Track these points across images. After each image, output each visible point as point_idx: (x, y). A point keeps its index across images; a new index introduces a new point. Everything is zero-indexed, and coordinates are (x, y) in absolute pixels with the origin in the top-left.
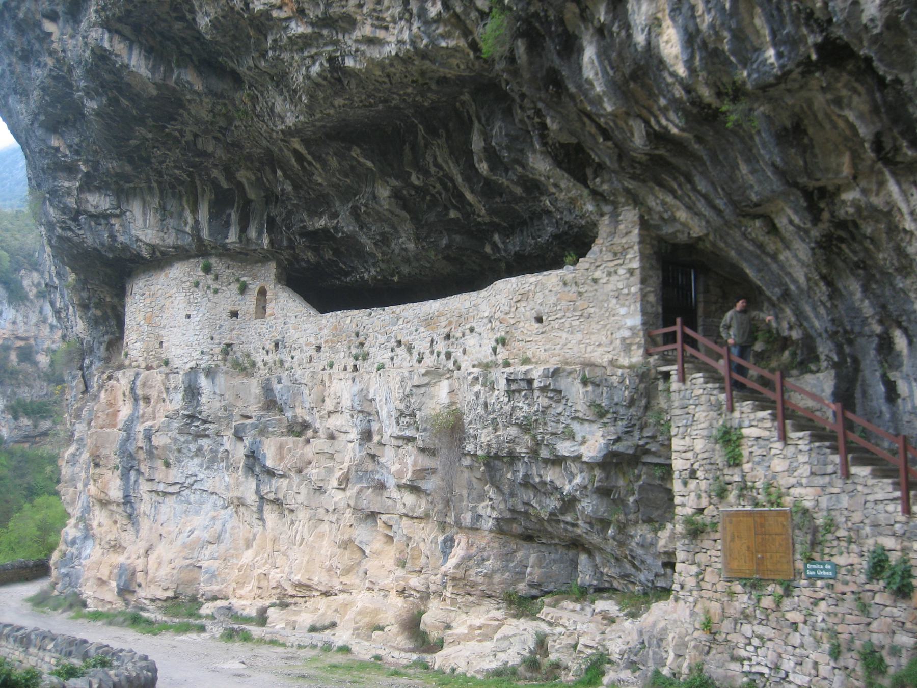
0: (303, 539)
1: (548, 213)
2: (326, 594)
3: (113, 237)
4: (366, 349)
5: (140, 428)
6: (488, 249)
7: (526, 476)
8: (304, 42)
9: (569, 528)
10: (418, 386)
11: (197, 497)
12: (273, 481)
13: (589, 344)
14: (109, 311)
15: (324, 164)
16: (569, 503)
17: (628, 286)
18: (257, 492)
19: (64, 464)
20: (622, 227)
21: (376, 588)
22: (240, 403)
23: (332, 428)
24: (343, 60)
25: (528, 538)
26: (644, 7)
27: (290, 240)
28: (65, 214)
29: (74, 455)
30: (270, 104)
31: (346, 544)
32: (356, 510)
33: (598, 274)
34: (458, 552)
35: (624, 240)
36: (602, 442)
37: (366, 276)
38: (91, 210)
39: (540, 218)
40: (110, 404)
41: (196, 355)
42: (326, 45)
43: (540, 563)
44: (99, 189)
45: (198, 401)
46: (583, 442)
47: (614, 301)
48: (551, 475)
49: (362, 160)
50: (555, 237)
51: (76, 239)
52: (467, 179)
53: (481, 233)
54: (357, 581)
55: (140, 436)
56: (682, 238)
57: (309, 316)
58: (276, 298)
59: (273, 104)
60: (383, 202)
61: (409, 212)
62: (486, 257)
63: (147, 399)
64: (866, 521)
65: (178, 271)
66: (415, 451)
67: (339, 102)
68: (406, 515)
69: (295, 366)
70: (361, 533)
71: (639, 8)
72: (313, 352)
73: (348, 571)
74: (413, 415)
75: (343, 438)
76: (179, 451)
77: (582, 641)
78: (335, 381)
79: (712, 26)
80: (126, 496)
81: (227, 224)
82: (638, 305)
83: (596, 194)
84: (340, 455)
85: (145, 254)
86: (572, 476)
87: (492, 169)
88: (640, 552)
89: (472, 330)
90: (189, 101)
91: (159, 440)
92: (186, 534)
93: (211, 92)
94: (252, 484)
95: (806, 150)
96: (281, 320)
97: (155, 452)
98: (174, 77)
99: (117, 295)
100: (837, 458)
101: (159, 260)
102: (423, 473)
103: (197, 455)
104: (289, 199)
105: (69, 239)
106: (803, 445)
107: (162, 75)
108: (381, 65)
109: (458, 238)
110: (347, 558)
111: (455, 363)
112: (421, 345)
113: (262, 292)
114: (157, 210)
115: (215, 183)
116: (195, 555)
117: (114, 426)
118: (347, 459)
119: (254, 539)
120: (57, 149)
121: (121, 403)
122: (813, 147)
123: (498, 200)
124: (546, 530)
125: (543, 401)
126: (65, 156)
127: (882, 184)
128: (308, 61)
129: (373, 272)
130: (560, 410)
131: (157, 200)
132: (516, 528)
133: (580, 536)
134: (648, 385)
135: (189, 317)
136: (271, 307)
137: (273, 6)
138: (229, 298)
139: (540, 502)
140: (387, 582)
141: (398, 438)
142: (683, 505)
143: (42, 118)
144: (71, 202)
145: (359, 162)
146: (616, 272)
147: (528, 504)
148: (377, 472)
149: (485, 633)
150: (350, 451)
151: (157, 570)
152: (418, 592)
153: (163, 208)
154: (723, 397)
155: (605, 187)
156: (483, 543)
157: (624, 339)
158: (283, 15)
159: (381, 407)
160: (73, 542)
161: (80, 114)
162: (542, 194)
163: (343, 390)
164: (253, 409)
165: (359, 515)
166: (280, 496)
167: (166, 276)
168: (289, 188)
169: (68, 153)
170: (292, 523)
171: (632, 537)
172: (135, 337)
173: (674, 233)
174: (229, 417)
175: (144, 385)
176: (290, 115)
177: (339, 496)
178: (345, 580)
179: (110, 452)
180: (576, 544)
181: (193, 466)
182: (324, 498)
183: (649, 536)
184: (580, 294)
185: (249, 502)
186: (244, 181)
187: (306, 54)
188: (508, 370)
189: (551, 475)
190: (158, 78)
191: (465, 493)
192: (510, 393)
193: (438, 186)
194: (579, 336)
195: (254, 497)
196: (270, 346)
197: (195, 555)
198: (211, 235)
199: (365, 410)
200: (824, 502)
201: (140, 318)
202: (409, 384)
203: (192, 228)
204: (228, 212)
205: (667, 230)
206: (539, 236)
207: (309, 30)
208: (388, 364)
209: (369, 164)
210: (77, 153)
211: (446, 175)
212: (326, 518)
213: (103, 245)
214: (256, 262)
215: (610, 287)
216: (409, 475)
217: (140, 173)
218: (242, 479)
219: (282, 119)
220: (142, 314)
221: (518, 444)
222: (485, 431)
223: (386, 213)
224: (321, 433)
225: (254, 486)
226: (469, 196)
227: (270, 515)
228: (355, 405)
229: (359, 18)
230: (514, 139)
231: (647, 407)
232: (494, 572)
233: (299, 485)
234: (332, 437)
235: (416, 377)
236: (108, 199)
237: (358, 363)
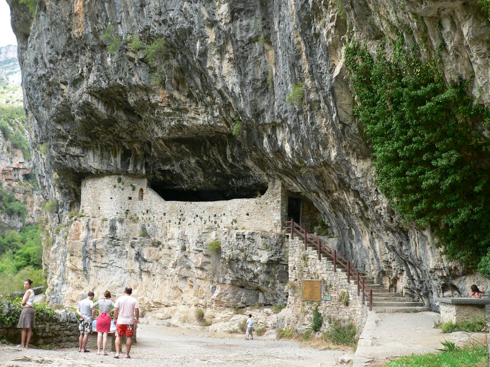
1: (252, 176)
2: (167, 306)
3: (80, 165)
4: (184, 216)
5: (91, 241)
6: (230, 183)
7: (242, 266)
8: (169, 114)
11: (114, 268)
12: (146, 264)
14: (72, 191)
15: (171, 149)
16: (256, 276)
17: (277, 206)
18: (140, 268)
19: (51, 253)
21: (186, 304)
23: (170, 245)
26: (281, 135)
27: (153, 171)
29: (56, 249)
31: (175, 288)
32: (179, 275)
33: (267, 201)
34: (218, 291)
36: (267, 256)
37: (183, 187)
38: (72, 153)
39: (249, 177)
40: (76, 231)
41: (115, 214)
44: (75, 146)
46: (261, 256)
48: (250, 266)
50: (254, 184)
51: (63, 164)
52: (224, 161)
54: (179, 302)
55: (91, 244)
56: (296, 191)
62: (230, 186)
63: (94, 230)
65: (106, 179)
67: (180, 133)
70: (181, 284)
72: (163, 216)
74: (202, 243)
75: (174, 249)
77: (259, 321)
79: (298, 149)
80: (84, 268)
81: (128, 163)
85: (93, 172)
86: (257, 267)
88: (279, 292)
89: (224, 214)
91: (99, 246)
94: (137, 264)
95: (324, 181)
98: (115, 113)
100: (333, 266)
101: (99, 175)
102: (205, 263)
104: (155, 158)
105: (60, 164)
106: (325, 261)
109: (219, 179)
112: (206, 218)
113: (142, 190)
114: (99, 156)
115: (124, 148)
117: (78, 239)
118: (176, 256)
120: (60, 130)
121: (81, 230)
125: (248, 242)
127: (343, 193)
129: (186, 186)
131: (99, 152)
132: (238, 284)
134: (282, 240)
136: (145, 196)
137: (159, 102)
138: (128, 191)
139: (246, 275)
140: (190, 302)
141: (196, 250)
142: (291, 278)
143: (55, 118)
144: (63, 150)
147: (243, 276)
149: (226, 319)
150: (177, 254)
154: (304, 245)
155: (271, 173)
156: (226, 288)
157: (275, 224)
158: (162, 105)
160: (57, 285)
161: (72, 118)
165: (180, 277)
167: (102, 181)
168: (156, 155)
170: (154, 280)
174: (128, 239)
175: (92, 224)
177: (173, 270)
179: (78, 251)
180: (258, 289)
181: (112, 257)
182: (166, 271)
183: (282, 287)
184: (262, 207)
185: (136, 271)
186: (136, 148)
188: (237, 231)
189: (250, 266)
190: (109, 113)
191: (221, 271)
192: (238, 239)
193: (213, 161)
194: (261, 221)
195: (138, 270)
196: (145, 212)
199: (183, 239)
201: (90, 196)
202: (201, 232)
203: (114, 164)
205: (290, 189)
207: (171, 111)
208: (193, 223)
209: (188, 150)
210: (69, 132)
211: (216, 158)
212: (167, 278)
213: (75, 167)
214: (139, 178)
216: (200, 264)
218: (133, 262)
219: (157, 134)
220: (90, 195)
224: (165, 246)
225: (138, 266)
226: (224, 166)
227: (145, 277)
230: (241, 154)
231: (281, 246)
232: (230, 298)
233: (157, 266)
234: (170, 248)
237: (181, 222)
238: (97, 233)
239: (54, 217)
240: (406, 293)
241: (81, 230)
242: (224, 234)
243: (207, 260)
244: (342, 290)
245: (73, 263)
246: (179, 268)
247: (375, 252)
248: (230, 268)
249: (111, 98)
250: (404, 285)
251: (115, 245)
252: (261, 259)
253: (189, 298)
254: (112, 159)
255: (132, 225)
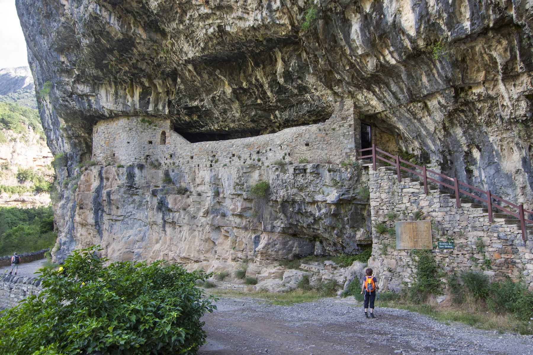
0: (186, 238)
2: (196, 262)
3: (90, 105)
4: (216, 158)
7: (299, 209)
9: (315, 231)
10: (245, 173)
12: (171, 214)
13: (331, 155)
16: (317, 220)
17: (349, 132)
18: (163, 219)
20: (345, 107)
21: (221, 258)
22: (154, 181)
24: (225, 27)
25: (294, 235)
27: (178, 111)
28: (65, 94)
29: (64, 205)
30: (181, 47)
31: (207, 240)
32: (212, 225)
33: (335, 126)
35: (346, 113)
36: (337, 195)
37: (212, 128)
38: (80, 93)
40: (87, 181)
41: (133, 159)
42: (217, 19)
43: (299, 246)
45: (134, 179)
46: (328, 195)
47: (342, 137)
49: (220, 76)
53: (270, 110)
58: (171, 136)
59: (183, 47)
60: (228, 95)
61: (238, 101)
62: (271, 121)
64: (469, 225)
65: (123, 122)
66: (242, 200)
67: (219, 47)
68: (236, 227)
69: (181, 165)
70: (213, 235)
71: (391, 5)
73: (207, 252)
76: (124, 201)
78: (201, 172)
81: (148, 102)
82: (353, 139)
83: (335, 94)
84: (204, 202)
85: (106, 114)
87: (285, 81)
90: (138, 43)
92: (127, 238)
93: (151, 39)
97: (112, 202)
98: (132, 31)
99: (88, 133)
101: (113, 116)
102: (244, 209)
103: (132, 203)
105: (66, 106)
106: (437, 195)
107: (126, 30)
108: (243, 30)
109: (260, 112)
110: (207, 246)
113: (164, 133)
116: (131, 247)
117: (89, 191)
118: (207, 204)
119: (160, 239)
120: (63, 62)
122: (468, 69)
123: (283, 95)
124: (303, 232)
125: (310, 178)
126: (67, 66)
128: (207, 27)
129: (216, 126)
130: (318, 181)
131: (113, 90)
132: (291, 231)
133: (319, 234)
135: (129, 143)
144: (69, 88)
145: (218, 77)
146: (343, 126)
147: (298, 221)
148: (221, 209)
150: (208, 201)
151: (112, 254)
152: (241, 259)
153: (116, 93)
155: (340, 90)
156: (275, 238)
157: (346, 153)
159: (225, 182)
160: (65, 243)
161: (78, 46)
162: (307, 93)
163: (205, 175)
164: (160, 184)
165: (213, 227)
166: (175, 220)
169: (69, 64)
170: (180, 232)
171: (345, 234)
172: (100, 151)
173: (368, 111)
174: (149, 187)
175: (106, 172)
176: (191, 52)
177: (203, 220)
178: (206, 255)
179: (89, 203)
181: (130, 208)
184: (327, 134)
185: (158, 223)
187: (206, 23)
189: (309, 209)
191: (268, 217)
194: (326, 151)
196: (169, 156)
197: (131, 247)
198: (140, 107)
199: (216, 183)
200: (447, 218)
204: (148, 97)
206: (300, 112)
207: (210, 11)
208: (229, 164)
215: (340, 132)
216: (239, 210)
217: (106, 77)
218: (155, 213)
219: (186, 54)
221: (297, 196)
222: (282, 190)
223: (228, 100)
224: (194, 193)
226: (269, 94)
227: (169, 230)
228: (212, 181)
229: (235, 8)
230: (300, 67)
232: (279, 250)
233: (184, 216)
234: (199, 195)
235: (245, 169)
236: (88, 88)
237: (213, 164)
238: (111, 182)
239: (63, 170)
241: (93, 180)
242: (275, 171)
243: (249, 205)
244: (475, 233)
246: (211, 217)
248: (283, 213)
251: (133, 195)
252: (328, 198)
253: (224, 251)
254: (129, 97)
255: (153, 171)
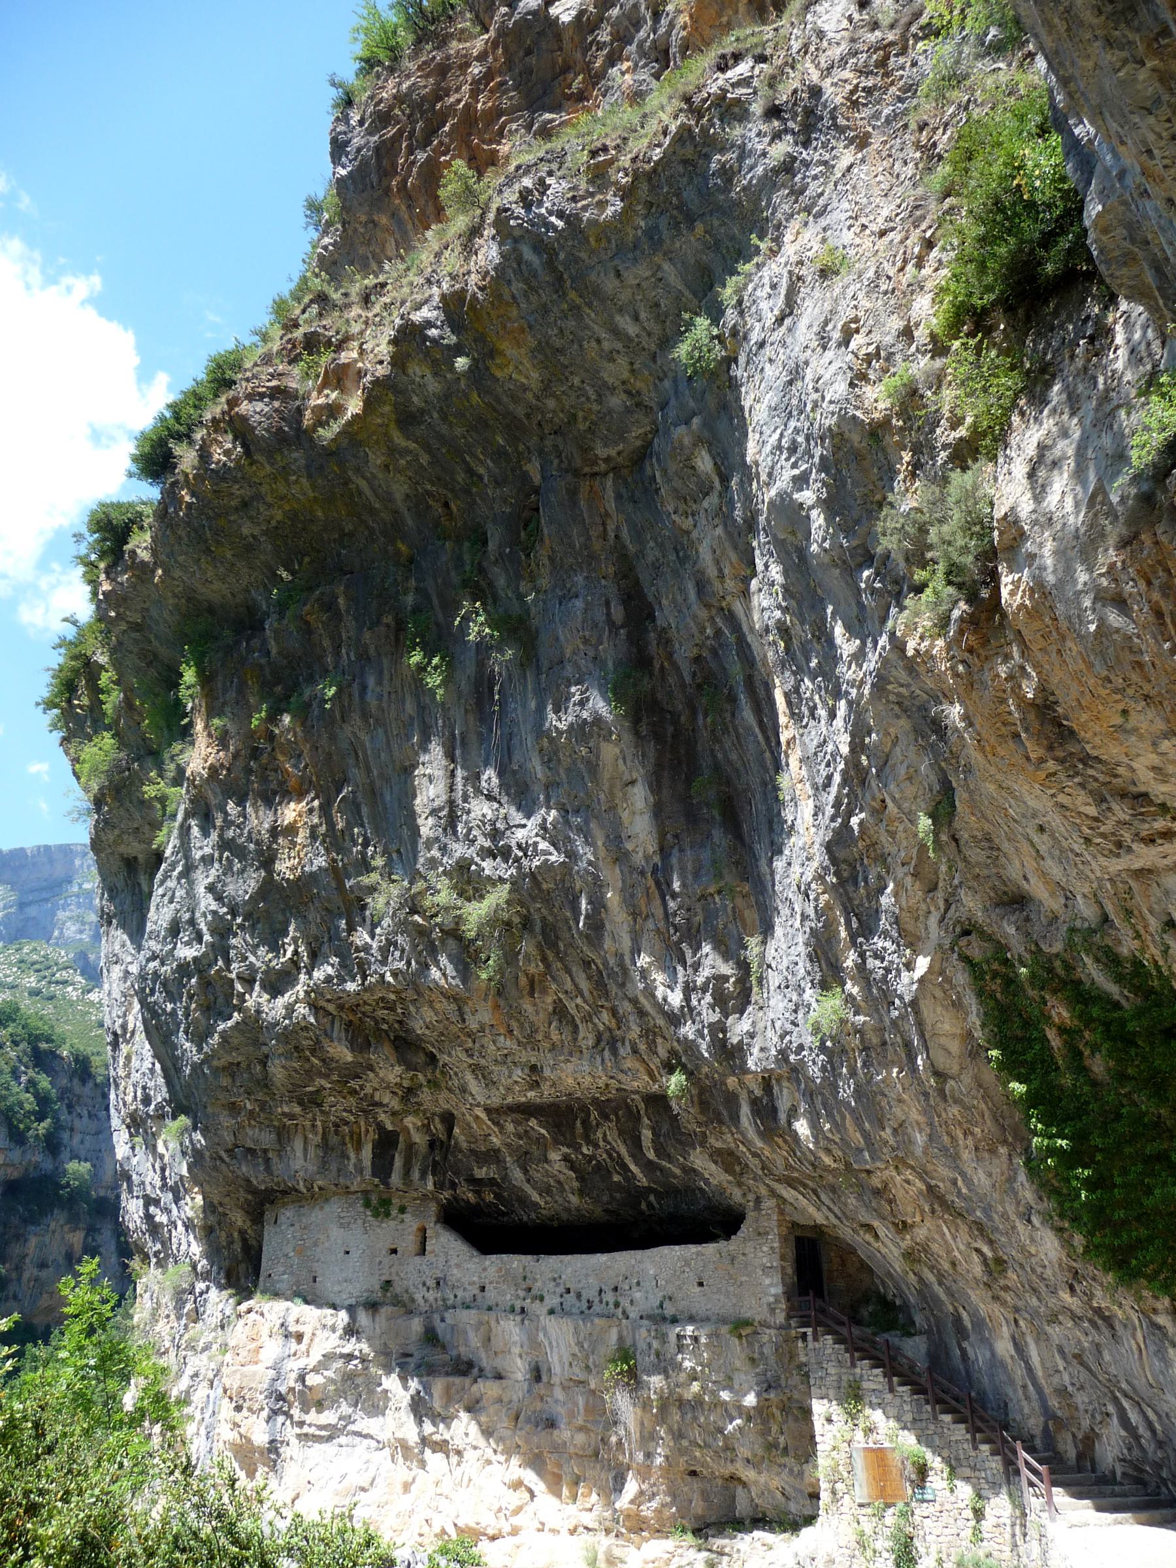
14: (236, 1235)
55: (294, 1376)
57: (472, 1256)
58: (437, 1236)
62: (642, 1213)
67: (531, 1094)
96: (442, 1259)
100: (929, 1408)
111: (624, 1312)
113: (423, 1230)
157: (769, 1304)
167: (322, 1208)
196: (431, 1283)
209: (543, 1131)
211: (613, 1148)
226: (633, 1167)
227: (434, 1459)
240: (1124, 1474)
245: (242, 1430)
247: (1030, 1369)
249: (363, 1013)
250: (1116, 1451)
